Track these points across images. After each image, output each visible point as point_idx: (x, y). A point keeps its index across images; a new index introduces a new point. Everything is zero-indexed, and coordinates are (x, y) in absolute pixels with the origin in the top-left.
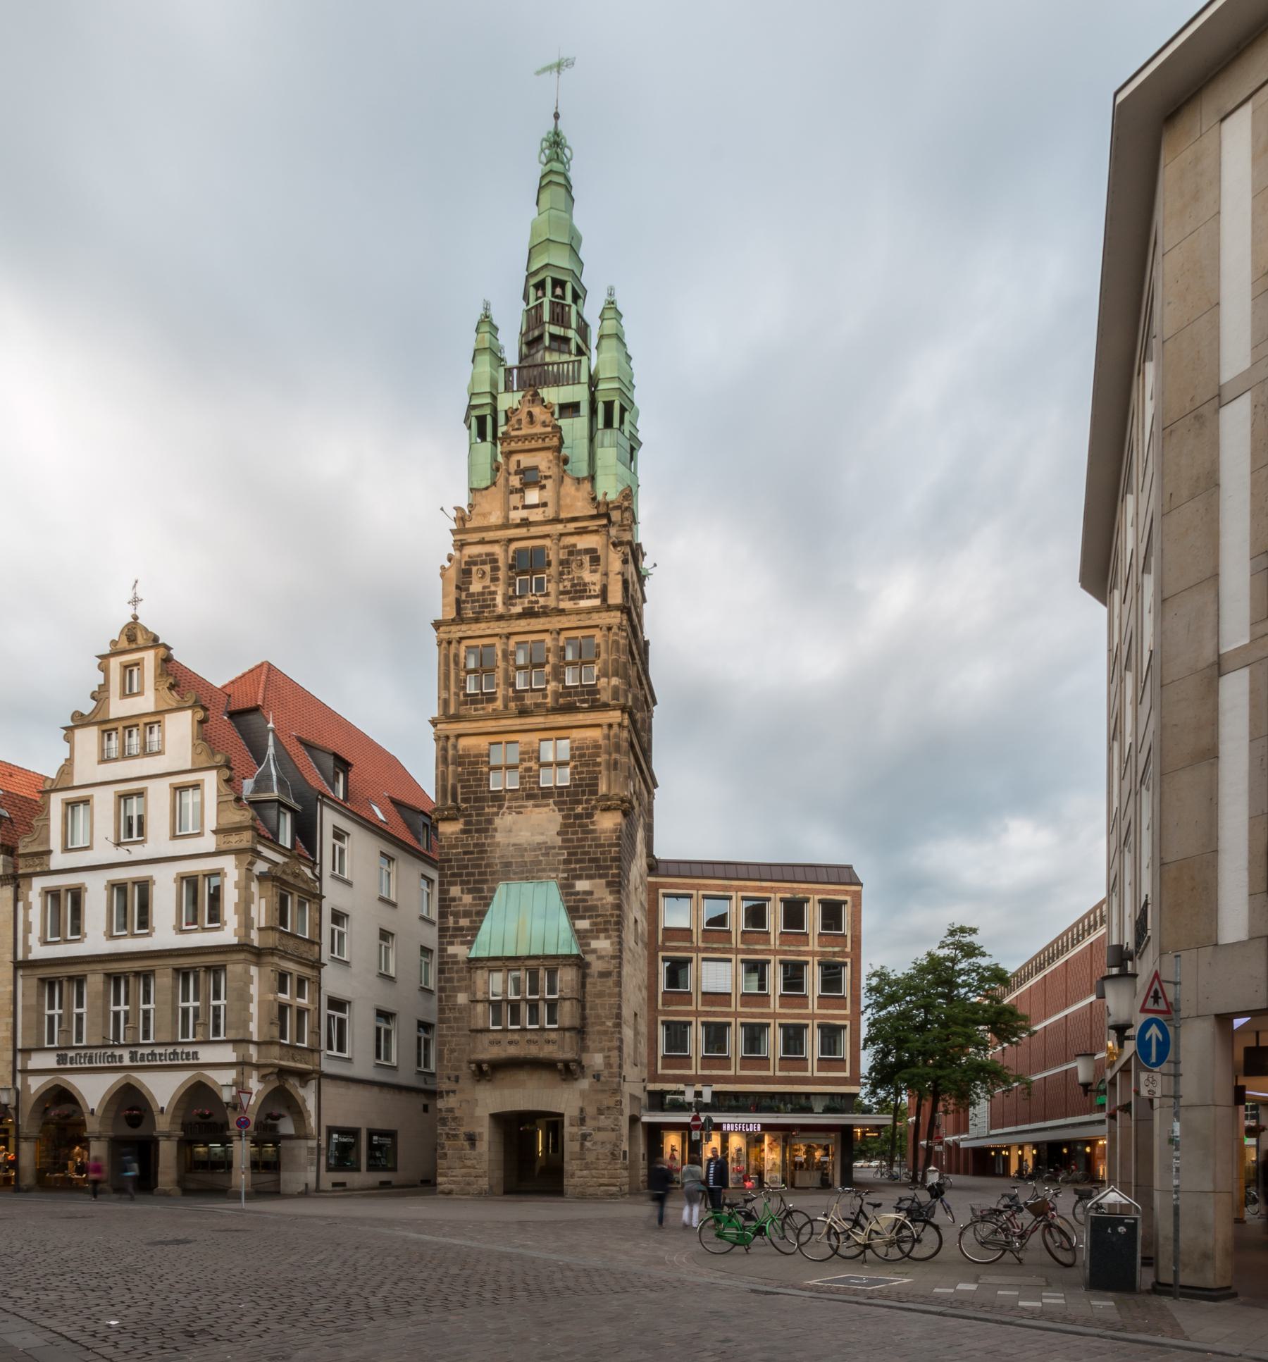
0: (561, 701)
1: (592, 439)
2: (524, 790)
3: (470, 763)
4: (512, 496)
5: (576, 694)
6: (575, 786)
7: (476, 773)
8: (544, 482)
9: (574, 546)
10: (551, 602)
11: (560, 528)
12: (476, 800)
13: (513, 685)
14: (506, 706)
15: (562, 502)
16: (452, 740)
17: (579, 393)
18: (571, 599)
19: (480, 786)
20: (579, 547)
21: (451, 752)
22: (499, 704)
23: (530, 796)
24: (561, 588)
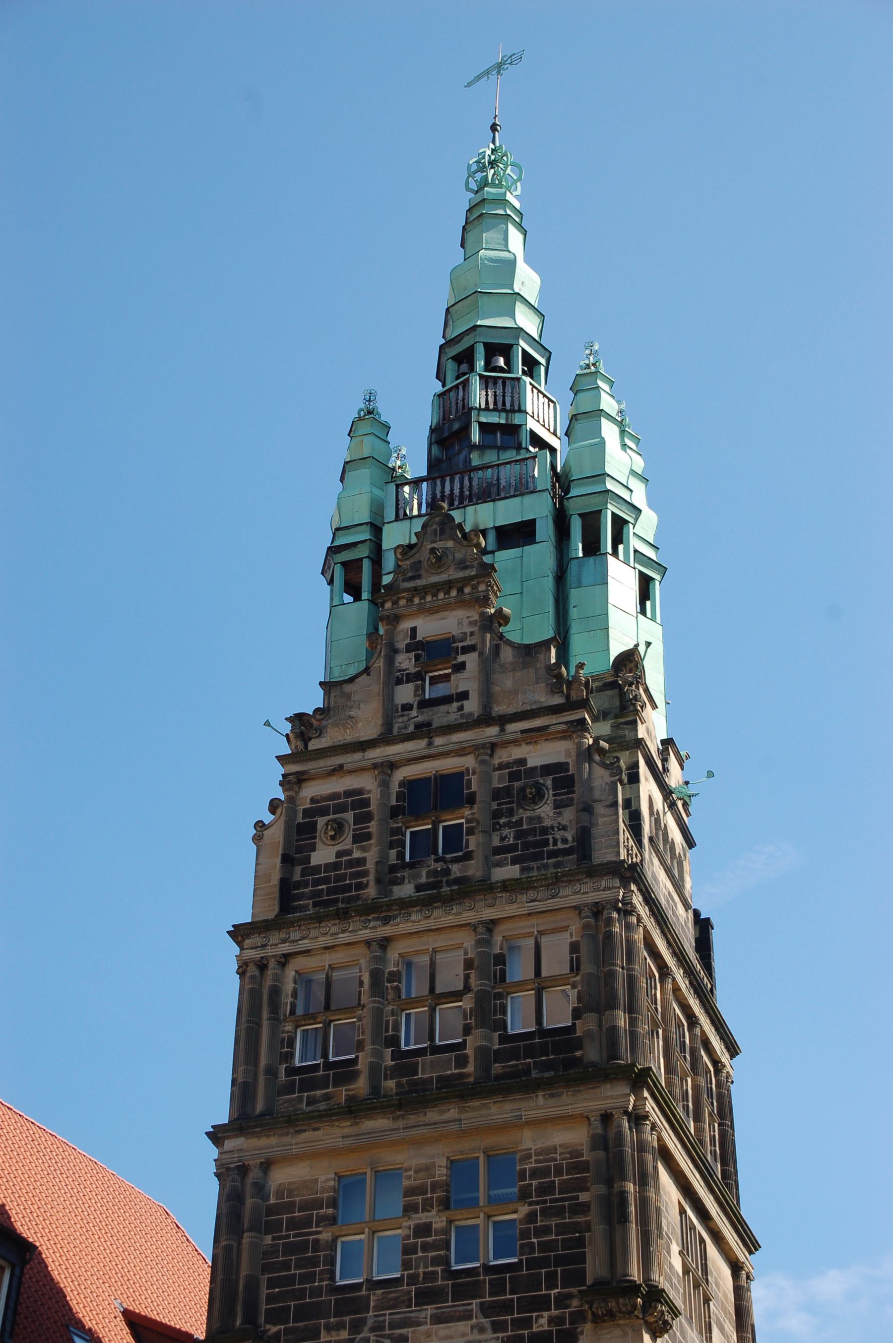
0: (497, 1068)
1: (561, 578)
2: (413, 1279)
3: (293, 1224)
4: (399, 688)
5: (530, 1052)
6: (532, 1264)
7: (302, 1247)
8: (461, 658)
9: (522, 762)
10: (474, 869)
11: (493, 731)
12: (302, 1313)
13: (393, 1041)
14: (375, 1089)
15: (496, 689)
16: (254, 1175)
17: (538, 508)
18: (514, 862)
19: (311, 1277)
20: (530, 764)
21: (249, 1202)
22: (361, 1086)
23: (426, 1297)
24: (496, 842)
